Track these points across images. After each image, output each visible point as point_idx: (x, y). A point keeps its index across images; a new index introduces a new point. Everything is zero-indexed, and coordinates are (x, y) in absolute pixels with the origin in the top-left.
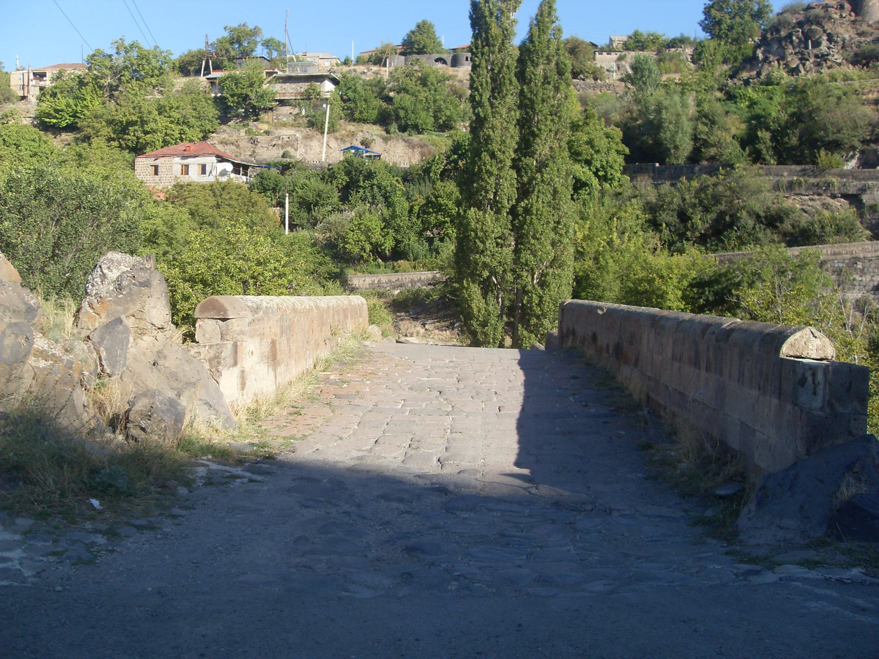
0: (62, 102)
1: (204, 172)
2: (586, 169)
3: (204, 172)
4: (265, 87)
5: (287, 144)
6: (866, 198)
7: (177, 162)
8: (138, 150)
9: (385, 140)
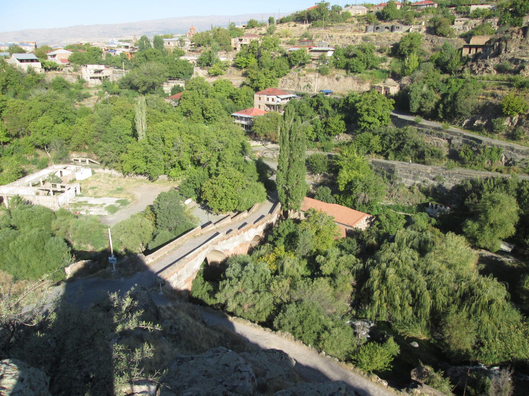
0: (243, 59)
1: (273, 100)
2: (373, 118)
3: (273, 100)
4: (308, 53)
5: (309, 81)
6: (452, 141)
7: (265, 97)
8: (257, 90)
9: (345, 77)
